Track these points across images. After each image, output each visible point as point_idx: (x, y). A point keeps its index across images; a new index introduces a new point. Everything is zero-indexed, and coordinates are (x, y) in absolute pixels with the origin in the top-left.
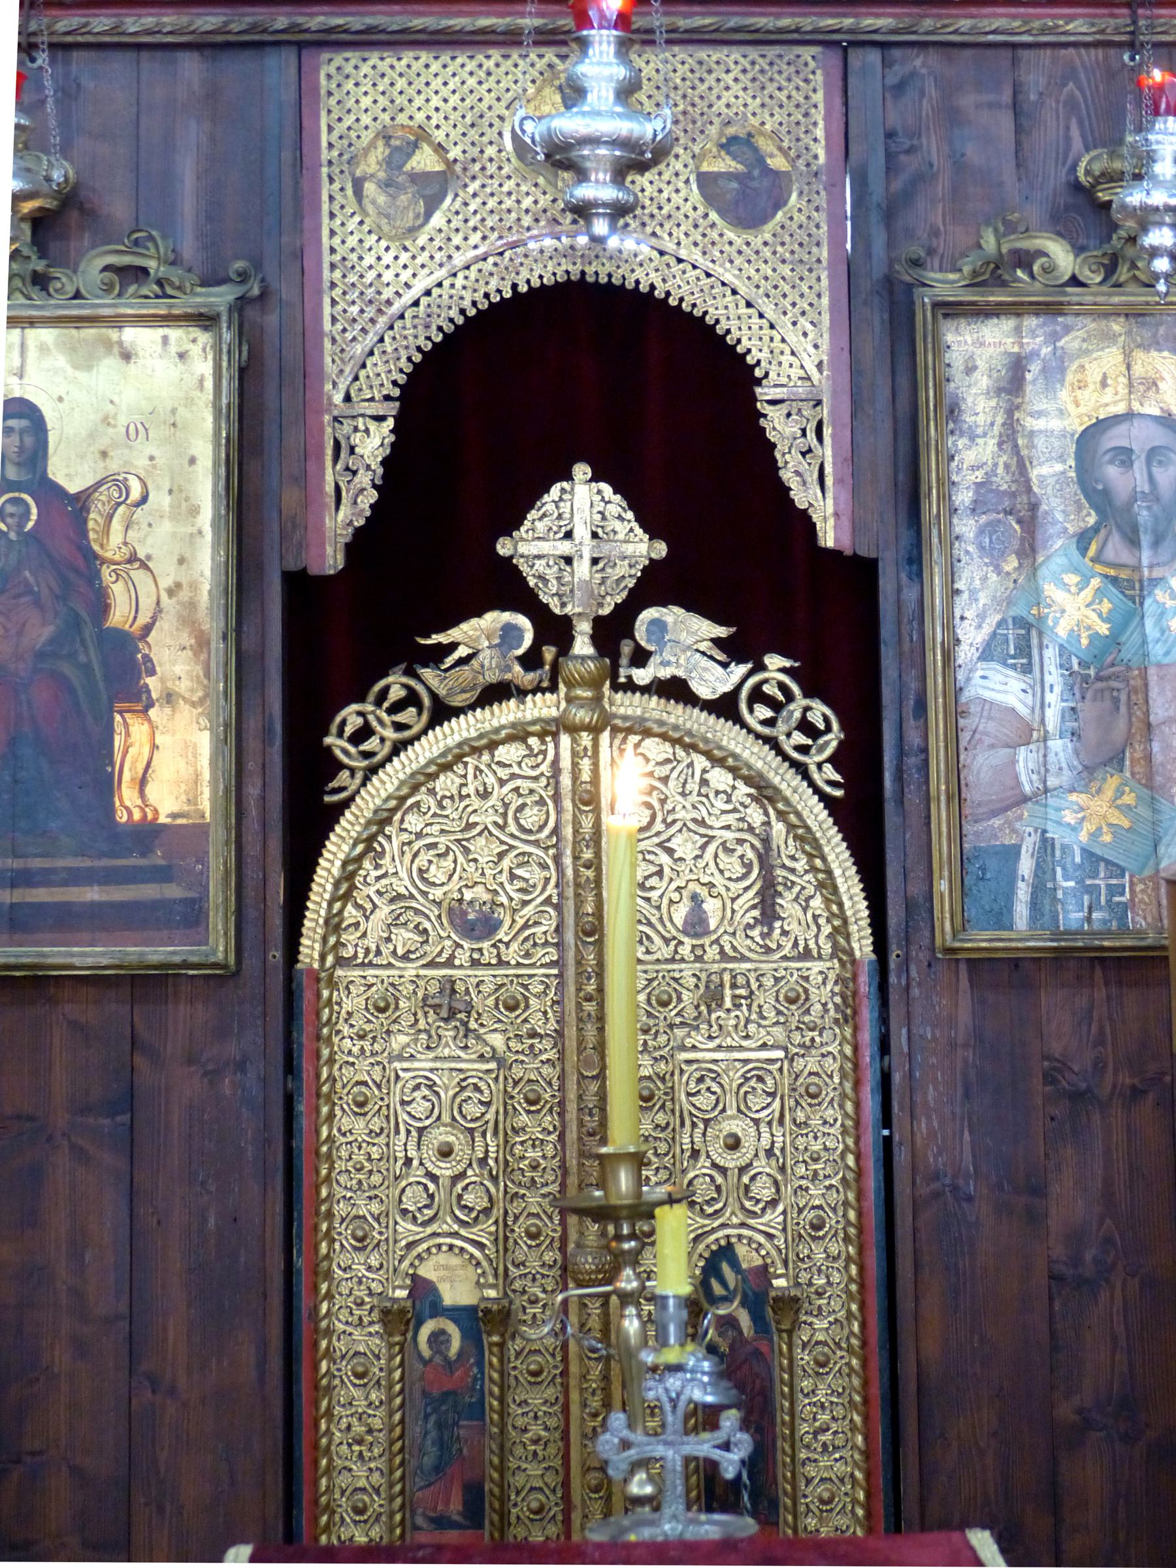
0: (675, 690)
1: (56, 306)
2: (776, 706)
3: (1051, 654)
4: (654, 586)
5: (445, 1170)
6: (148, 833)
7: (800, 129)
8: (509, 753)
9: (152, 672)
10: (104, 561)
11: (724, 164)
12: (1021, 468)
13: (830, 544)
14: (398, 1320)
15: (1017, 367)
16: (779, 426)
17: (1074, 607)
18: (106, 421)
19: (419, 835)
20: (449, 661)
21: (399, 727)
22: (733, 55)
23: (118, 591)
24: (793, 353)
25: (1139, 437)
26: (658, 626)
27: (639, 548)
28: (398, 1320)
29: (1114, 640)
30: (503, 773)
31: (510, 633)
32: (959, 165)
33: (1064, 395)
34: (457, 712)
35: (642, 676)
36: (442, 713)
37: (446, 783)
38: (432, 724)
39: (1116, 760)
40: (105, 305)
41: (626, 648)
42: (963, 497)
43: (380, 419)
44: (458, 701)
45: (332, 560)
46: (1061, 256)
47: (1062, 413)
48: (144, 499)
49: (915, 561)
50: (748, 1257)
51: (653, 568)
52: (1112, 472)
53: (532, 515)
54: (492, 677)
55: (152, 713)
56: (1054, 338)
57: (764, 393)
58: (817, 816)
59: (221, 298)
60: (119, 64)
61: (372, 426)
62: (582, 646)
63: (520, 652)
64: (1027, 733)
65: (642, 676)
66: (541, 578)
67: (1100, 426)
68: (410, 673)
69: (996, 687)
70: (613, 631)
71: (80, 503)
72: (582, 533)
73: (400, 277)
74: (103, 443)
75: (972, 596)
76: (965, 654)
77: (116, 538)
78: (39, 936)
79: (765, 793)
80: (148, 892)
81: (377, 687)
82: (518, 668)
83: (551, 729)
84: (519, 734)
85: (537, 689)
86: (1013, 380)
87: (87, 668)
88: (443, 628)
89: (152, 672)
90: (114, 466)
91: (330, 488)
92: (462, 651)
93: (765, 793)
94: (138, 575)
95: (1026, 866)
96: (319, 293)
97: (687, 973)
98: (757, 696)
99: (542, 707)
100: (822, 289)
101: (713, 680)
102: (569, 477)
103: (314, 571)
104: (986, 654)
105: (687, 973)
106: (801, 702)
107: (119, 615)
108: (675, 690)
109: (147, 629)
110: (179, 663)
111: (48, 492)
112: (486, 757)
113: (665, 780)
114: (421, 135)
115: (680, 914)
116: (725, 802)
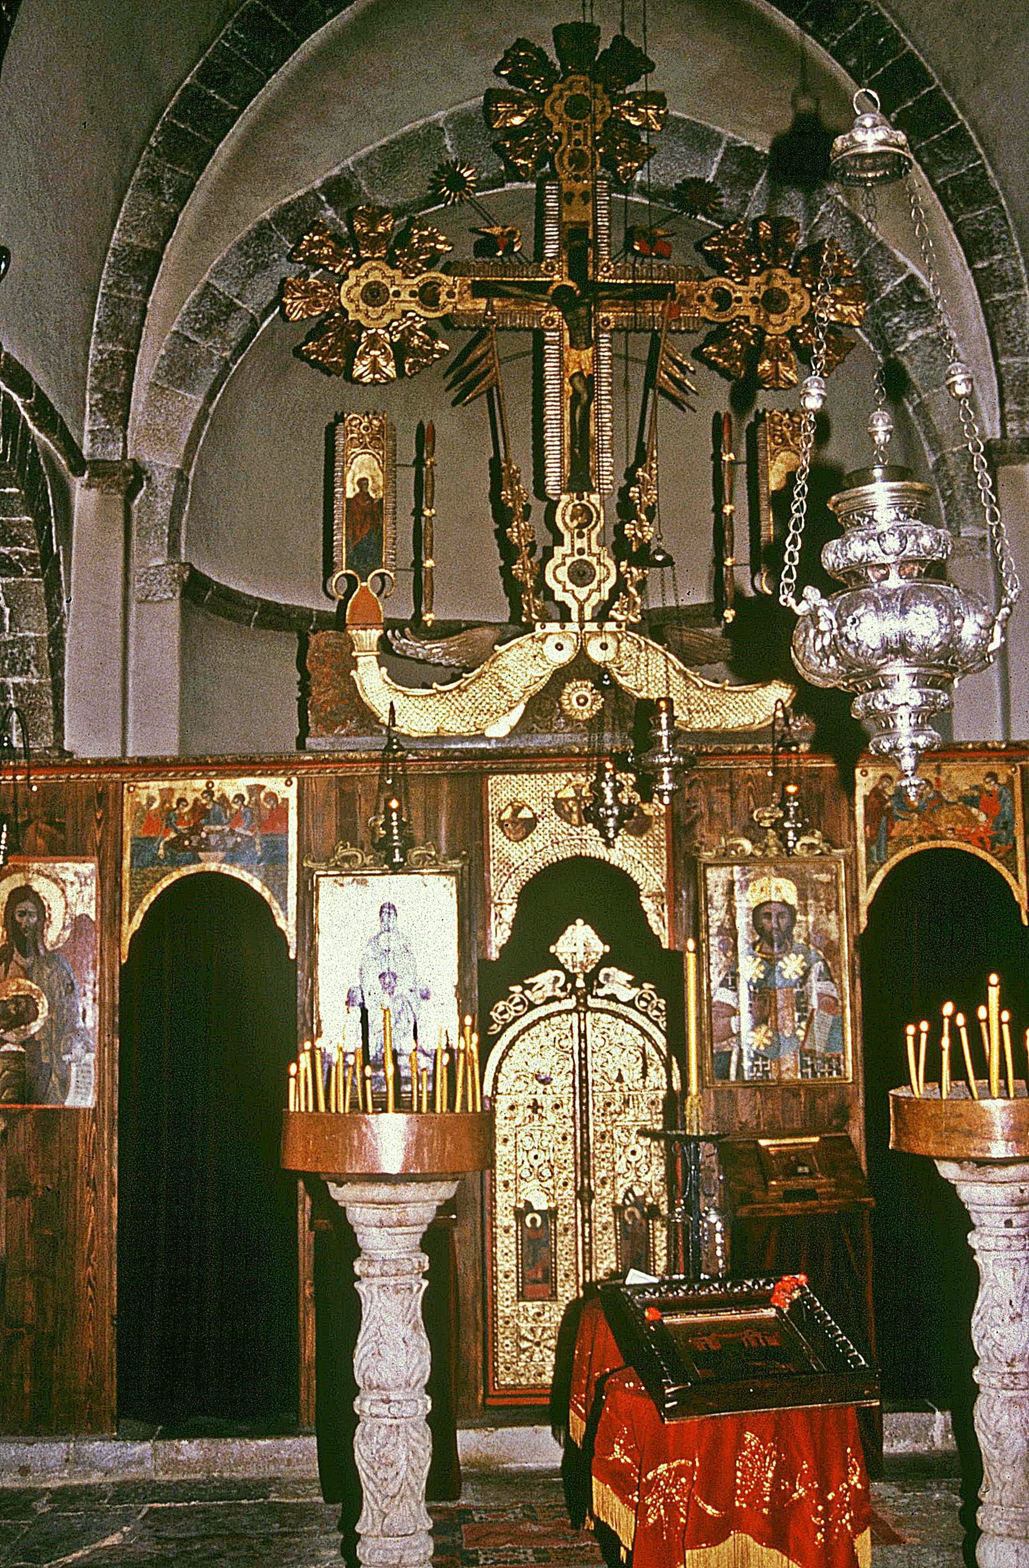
0: (612, 998)
2: (648, 1002)
4: (605, 961)
5: (536, 1163)
13: (665, 946)
31: (557, 979)
34: (537, 1006)
35: (601, 992)
36: (532, 1006)
44: (538, 1002)
45: (494, 955)
52: (765, 921)
54: (550, 994)
59: (456, 864)
62: (580, 983)
65: (601, 992)
70: (591, 978)
72: (580, 944)
79: (644, 1033)
88: (532, 976)
93: (644, 1033)
95: (734, 1058)
98: (641, 998)
101: (626, 994)
104: (721, 985)
115: (615, 1075)
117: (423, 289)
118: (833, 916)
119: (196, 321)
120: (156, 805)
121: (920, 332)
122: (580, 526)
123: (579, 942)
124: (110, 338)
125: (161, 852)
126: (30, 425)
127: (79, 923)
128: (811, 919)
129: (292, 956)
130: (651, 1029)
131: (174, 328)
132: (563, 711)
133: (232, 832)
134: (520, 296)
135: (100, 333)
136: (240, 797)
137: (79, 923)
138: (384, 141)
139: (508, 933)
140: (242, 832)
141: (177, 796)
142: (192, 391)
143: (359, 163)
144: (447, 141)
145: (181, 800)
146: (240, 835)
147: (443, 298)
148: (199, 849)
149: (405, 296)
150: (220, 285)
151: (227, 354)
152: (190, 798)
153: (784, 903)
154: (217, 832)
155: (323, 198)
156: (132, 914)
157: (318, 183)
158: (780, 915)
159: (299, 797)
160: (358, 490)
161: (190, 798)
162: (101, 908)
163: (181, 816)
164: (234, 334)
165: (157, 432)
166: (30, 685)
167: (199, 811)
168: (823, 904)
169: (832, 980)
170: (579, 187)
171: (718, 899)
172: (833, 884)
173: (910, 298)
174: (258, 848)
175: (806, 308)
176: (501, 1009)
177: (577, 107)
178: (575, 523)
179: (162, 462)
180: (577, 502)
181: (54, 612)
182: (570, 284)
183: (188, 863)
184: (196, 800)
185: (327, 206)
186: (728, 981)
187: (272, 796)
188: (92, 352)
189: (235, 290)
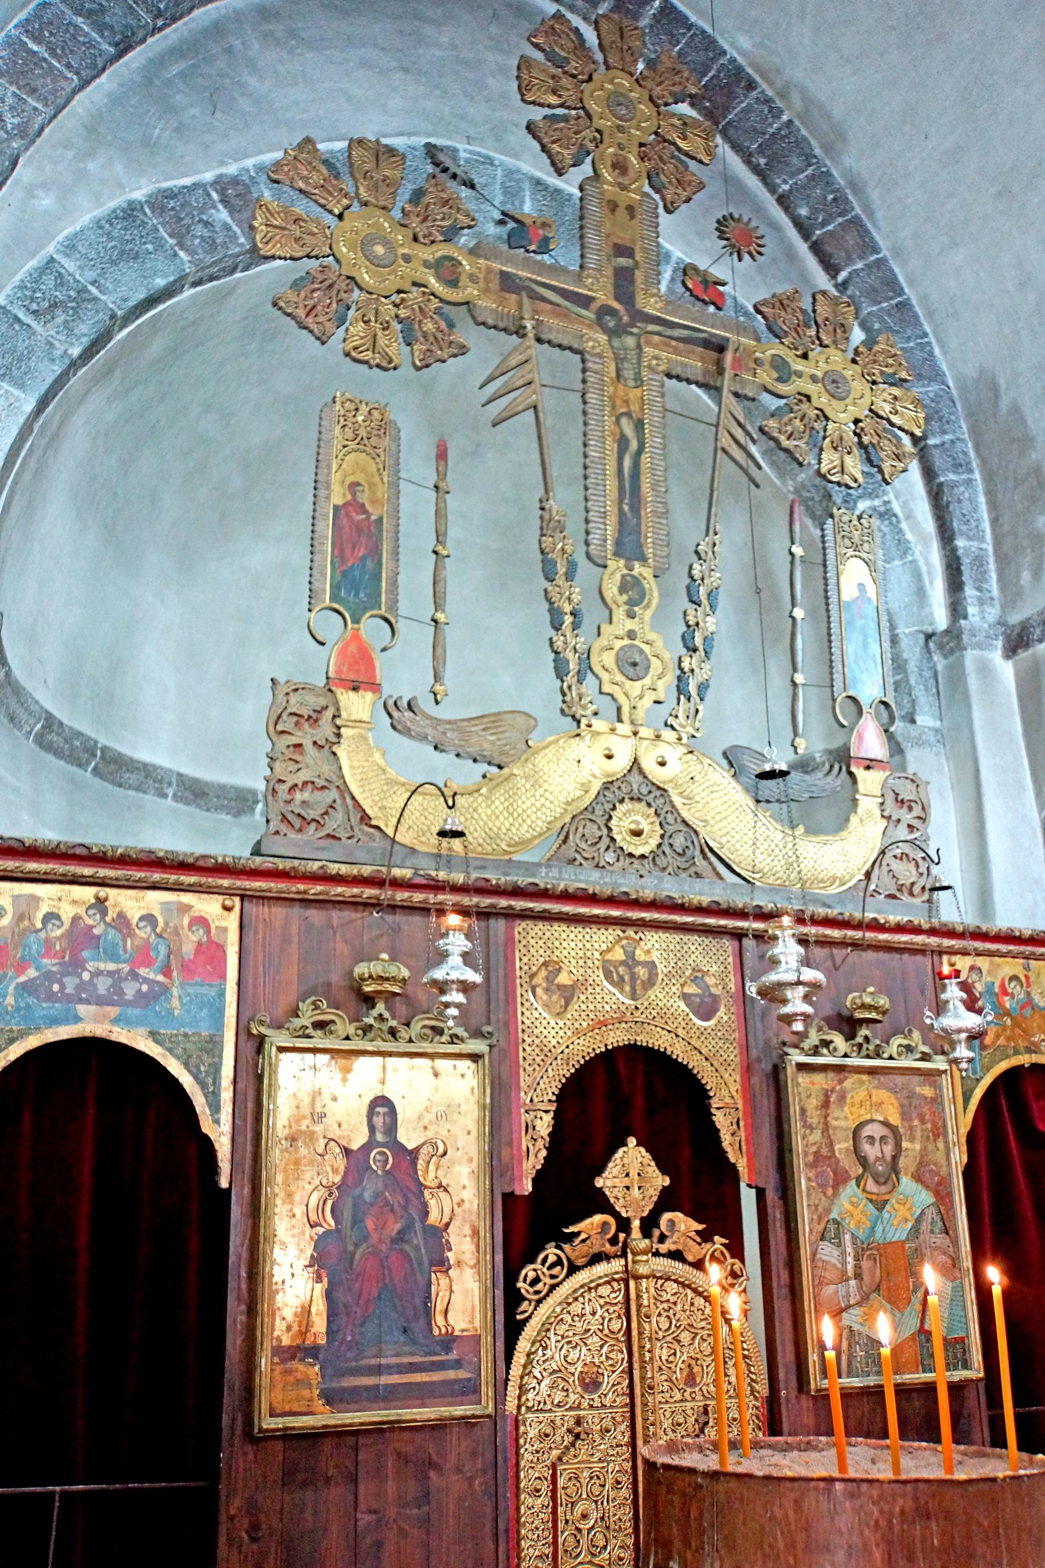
1: (402, 1047)
3: (848, 1237)
4: (666, 1201)
6: (449, 1341)
9: (450, 1249)
10: (426, 1187)
12: (831, 1145)
16: (720, 1120)
18: (427, 1110)
19: (563, 1337)
20: (577, 1241)
21: (552, 1277)
23: (432, 1203)
26: (672, 1223)
30: (602, 1301)
33: (846, 1109)
36: (573, 1269)
38: (569, 1274)
41: (656, 1233)
43: (547, 1112)
44: (580, 1262)
47: (846, 1118)
48: (445, 1153)
51: (664, 1190)
53: (611, 1165)
54: (596, 1250)
55: (451, 1272)
56: (841, 1082)
57: (715, 1103)
59: (478, 1046)
61: (543, 1115)
63: (609, 1236)
65: (663, 1248)
66: (616, 1198)
68: (558, 1247)
70: (649, 1224)
71: (414, 1153)
73: (556, 1039)
74: (426, 1121)
77: (431, 1175)
78: (393, 1404)
80: (451, 1374)
81: (541, 1256)
82: (608, 1245)
85: (616, 1256)
87: (417, 1248)
89: (450, 1249)
90: (430, 1134)
91: (524, 1148)
92: (583, 1236)
94: (442, 1195)
96: (517, 1045)
102: (626, 1145)
103: (518, 1192)
106: (730, 1261)
107: (434, 1217)
108: (676, 1255)
109: (447, 1225)
111: (399, 1149)
112: (593, 1294)
113: (675, 1303)
119: (32, 300)
123: (631, 1174)
125: (10, 1000)
128: (918, 1147)
129: (224, 1183)
132: (613, 840)
133: (134, 975)
134: (558, 305)
136: (149, 919)
139: (544, 1153)
140: (152, 976)
141: (44, 909)
142: (22, 387)
143: (260, 168)
145: (51, 917)
146: (146, 980)
147: (464, 280)
148: (69, 999)
150: (70, 265)
151: (75, 351)
153: (886, 1124)
154: (110, 974)
155: (215, 196)
157: (209, 176)
158: (883, 1139)
159: (241, 927)
160: (349, 497)
161: (67, 912)
163: (48, 943)
164: (86, 329)
168: (929, 1126)
169: (947, 1233)
174: (175, 1002)
176: (531, 1275)
178: (625, 597)
180: (625, 571)
182: (616, 305)
183: (54, 1022)
184: (76, 919)
185: (220, 207)
187: (201, 922)
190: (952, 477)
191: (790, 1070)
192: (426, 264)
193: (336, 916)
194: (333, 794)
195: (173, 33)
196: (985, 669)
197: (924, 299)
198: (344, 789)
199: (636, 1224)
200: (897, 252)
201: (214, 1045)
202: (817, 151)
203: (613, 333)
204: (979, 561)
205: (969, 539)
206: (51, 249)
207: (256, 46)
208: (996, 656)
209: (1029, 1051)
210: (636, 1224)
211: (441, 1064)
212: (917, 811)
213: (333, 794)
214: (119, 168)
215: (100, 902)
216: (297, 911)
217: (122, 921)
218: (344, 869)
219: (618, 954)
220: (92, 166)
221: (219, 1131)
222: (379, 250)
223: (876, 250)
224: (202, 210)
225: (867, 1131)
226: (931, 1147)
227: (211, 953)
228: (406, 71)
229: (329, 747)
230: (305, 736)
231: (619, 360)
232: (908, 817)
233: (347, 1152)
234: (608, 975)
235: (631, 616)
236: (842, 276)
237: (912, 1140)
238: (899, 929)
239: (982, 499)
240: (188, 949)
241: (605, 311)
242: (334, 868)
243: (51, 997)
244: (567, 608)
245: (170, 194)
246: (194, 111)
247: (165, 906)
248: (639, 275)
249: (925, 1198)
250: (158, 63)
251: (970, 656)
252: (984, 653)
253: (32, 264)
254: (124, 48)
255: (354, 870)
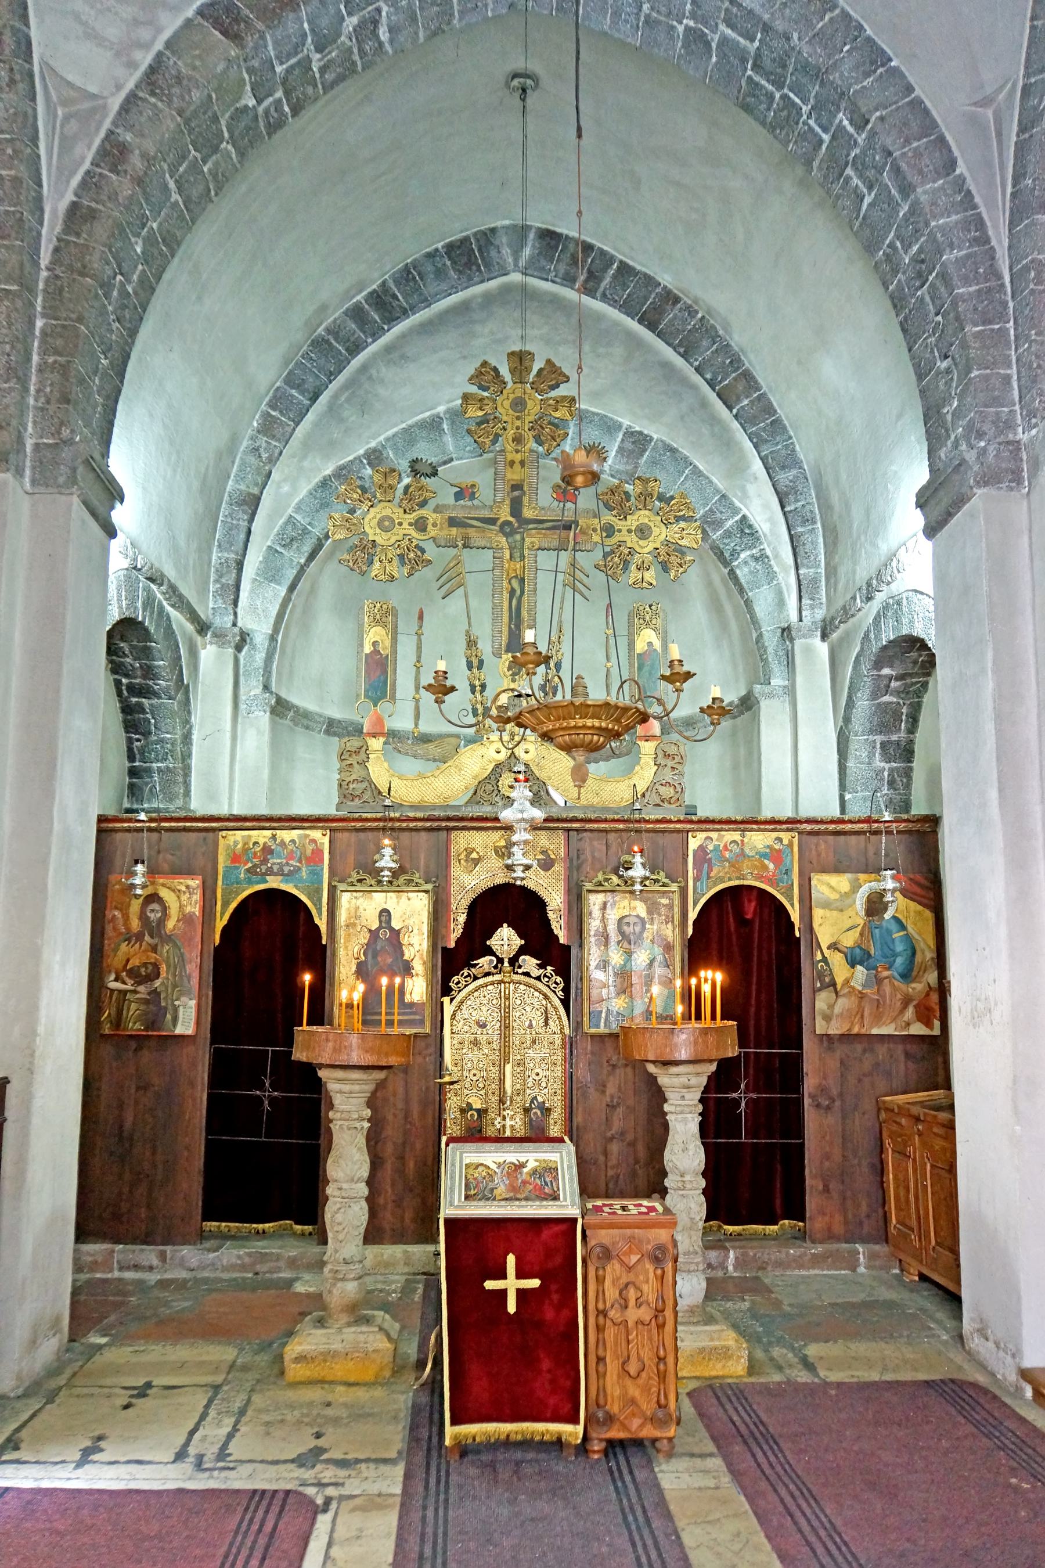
0: (527, 974)
1: (394, 888)
4: (522, 951)
6: (412, 1005)
7: (558, 849)
8: (490, 987)
11: (541, 857)
14: (463, 1111)
15: (605, 904)
16: (551, 916)
17: (616, 958)
22: (543, 832)
24: (555, 900)
25: (632, 920)
27: (518, 942)
28: (463, 1111)
29: (625, 965)
31: (491, 961)
32: (593, 857)
36: (476, 978)
37: (476, 994)
39: (624, 992)
40: (405, 888)
42: (592, 933)
45: (452, 945)
46: (615, 879)
49: (581, 946)
50: (540, 1099)
58: (558, 1003)
59: (429, 887)
60: (407, 834)
62: (506, 964)
64: (605, 986)
67: (623, 917)
69: (598, 975)
70: (513, 961)
71: (398, 932)
73: (469, 882)
75: (593, 954)
76: (592, 968)
79: (546, 997)
83: (500, 982)
84: (492, 983)
86: (604, 907)
93: (546, 997)
97: (528, 1037)
99: (497, 977)
100: (561, 886)
101: (536, 972)
105: (528, 1037)
107: (406, 957)
108: (527, 974)
110: (418, 967)
111: (392, 929)
114: (474, 850)
116: (537, 999)
117: (417, 521)
118: (670, 925)
120: (240, 846)
121: (748, 553)
122: (514, 674)
123: (506, 939)
124: (226, 550)
126: (165, 603)
127: (186, 919)
128: (655, 927)
130: (551, 995)
131: (269, 543)
135: (219, 546)
136: (293, 841)
137: (186, 919)
138: (404, 425)
142: (279, 584)
143: (387, 439)
144: (445, 426)
147: (430, 527)
148: (265, 874)
149: (405, 525)
150: (298, 517)
151: (302, 561)
152: (261, 841)
153: (638, 916)
156: (223, 914)
157: (361, 452)
161: (261, 841)
162: (204, 909)
163: (255, 853)
164: (307, 548)
165: (257, 610)
166: (168, 768)
167: (267, 850)
170: (518, 457)
171: (596, 913)
172: (670, 907)
173: (742, 531)
175: (663, 536)
177: (519, 404)
179: (260, 627)
181: (187, 722)
182: (511, 519)
183: (258, 883)
186: (598, 966)
187: (314, 841)
188: (214, 558)
189: (308, 520)
190: (800, 529)
191: (584, 892)
192: (410, 524)
193: (370, 834)
194: (366, 784)
195: (342, 378)
196: (808, 650)
197: (787, 418)
198: (371, 782)
199: (506, 961)
200: (771, 390)
201: (319, 891)
202: (721, 332)
203: (507, 535)
204: (815, 581)
205: (808, 567)
206: (290, 511)
207: (384, 370)
208: (817, 641)
209: (739, 878)
210: (506, 961)
211: (410, 895)
212: (678, 759)
213: (366, 784)
214: (318, 461)
215: (274, 837)
216: (354, 834)
217: (283, 844)
218: (369, 816)
219: (503, 843)
220: (306, 464)
221: (322, 923)
222: (387, 523)
223: (758, 389)
224: (358, 472)
225: (626, 920)
226: (663, 927)
227: (318, 852)
228: (464, 357)
229: (363, 764)
230: (353, 760)
231: (511, 549)
232: (670, 763)
233: (370, 931)
234: (496, 852)
235: (514, 681)
236: (735, 411)
237: (652, 924)
238: (658, 821)
239: (821, 540)
240: (309, 853)
241: (507, 523)
242: (365, 815)
243: (257, 873)
244: (477, 683)
245: (342, 468)
246: (353, 418)
247: (300, 836)
248: (526, 499)
249: (658, 950)
250: (336, 396)
251: (798, 643)
252: (808, 641)
253: (281, 522)
254: (314, 398)
255: (374, 816)
